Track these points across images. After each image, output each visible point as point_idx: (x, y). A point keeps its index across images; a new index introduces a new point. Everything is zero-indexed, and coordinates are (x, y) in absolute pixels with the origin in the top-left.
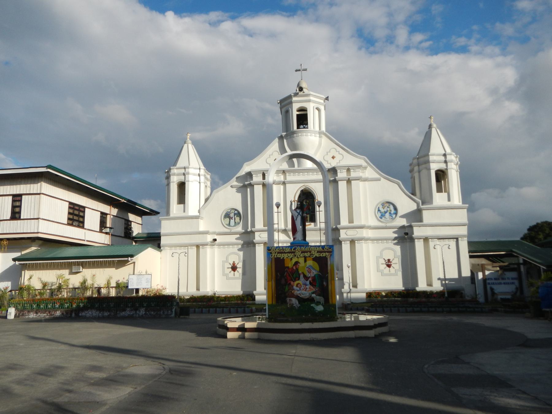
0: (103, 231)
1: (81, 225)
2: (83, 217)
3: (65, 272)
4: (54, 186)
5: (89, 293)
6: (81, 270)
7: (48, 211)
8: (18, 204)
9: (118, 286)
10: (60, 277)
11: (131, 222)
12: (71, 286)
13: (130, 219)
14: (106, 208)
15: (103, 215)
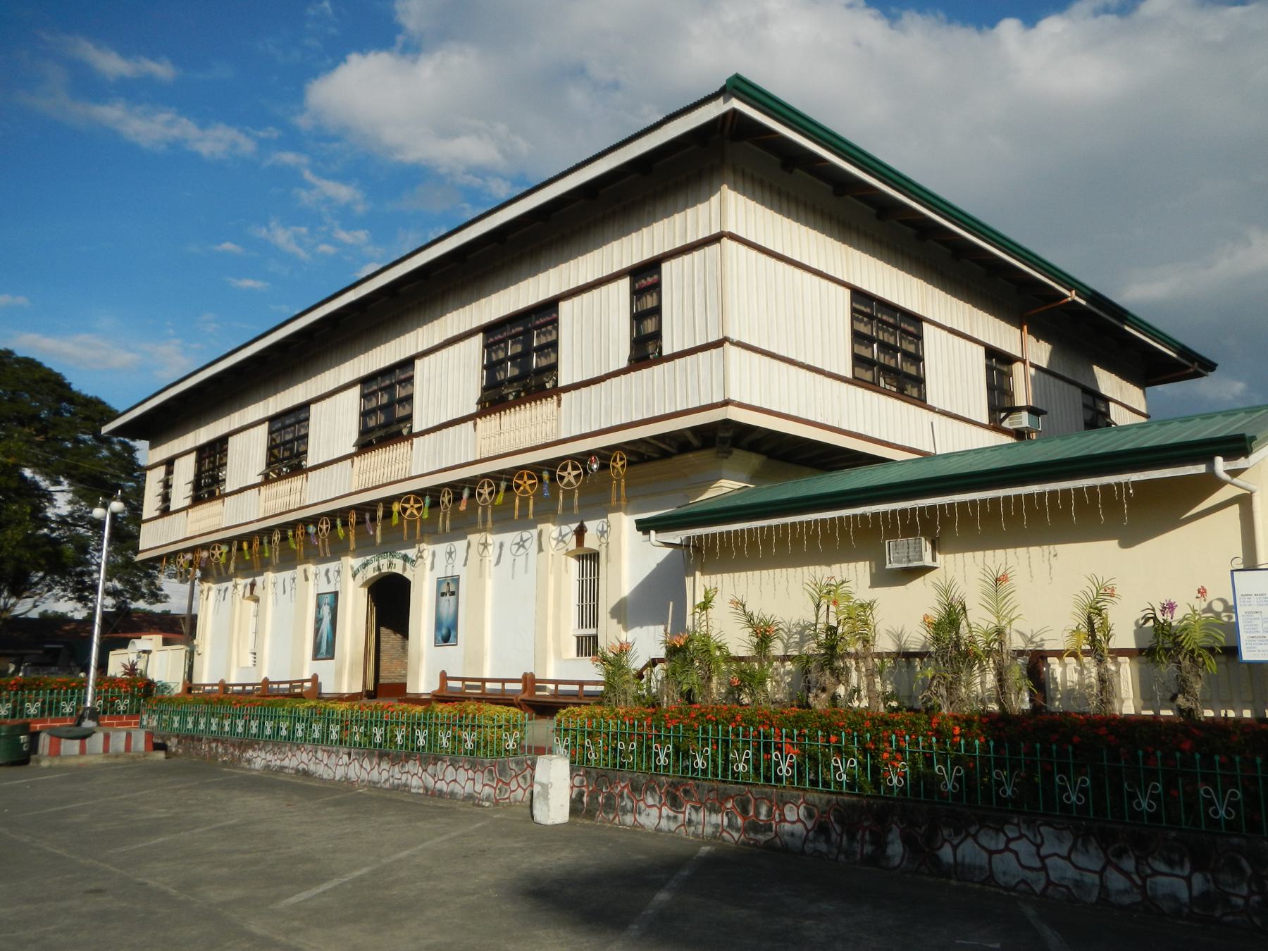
0: (1006, 424)
1: (915, 393)
2: (917, 358)
3: (855, 576)
4: (780, 211)
5: (982, 683)
6: (927, 560)
7: (766, 314)
8: (650, 302)
9: (1160, 645)
10: (827, 594)
11: (1106, 400)
12: (885, 644)
13: (1103, 391)
14: (1007, 337)
15: (998, 361)
